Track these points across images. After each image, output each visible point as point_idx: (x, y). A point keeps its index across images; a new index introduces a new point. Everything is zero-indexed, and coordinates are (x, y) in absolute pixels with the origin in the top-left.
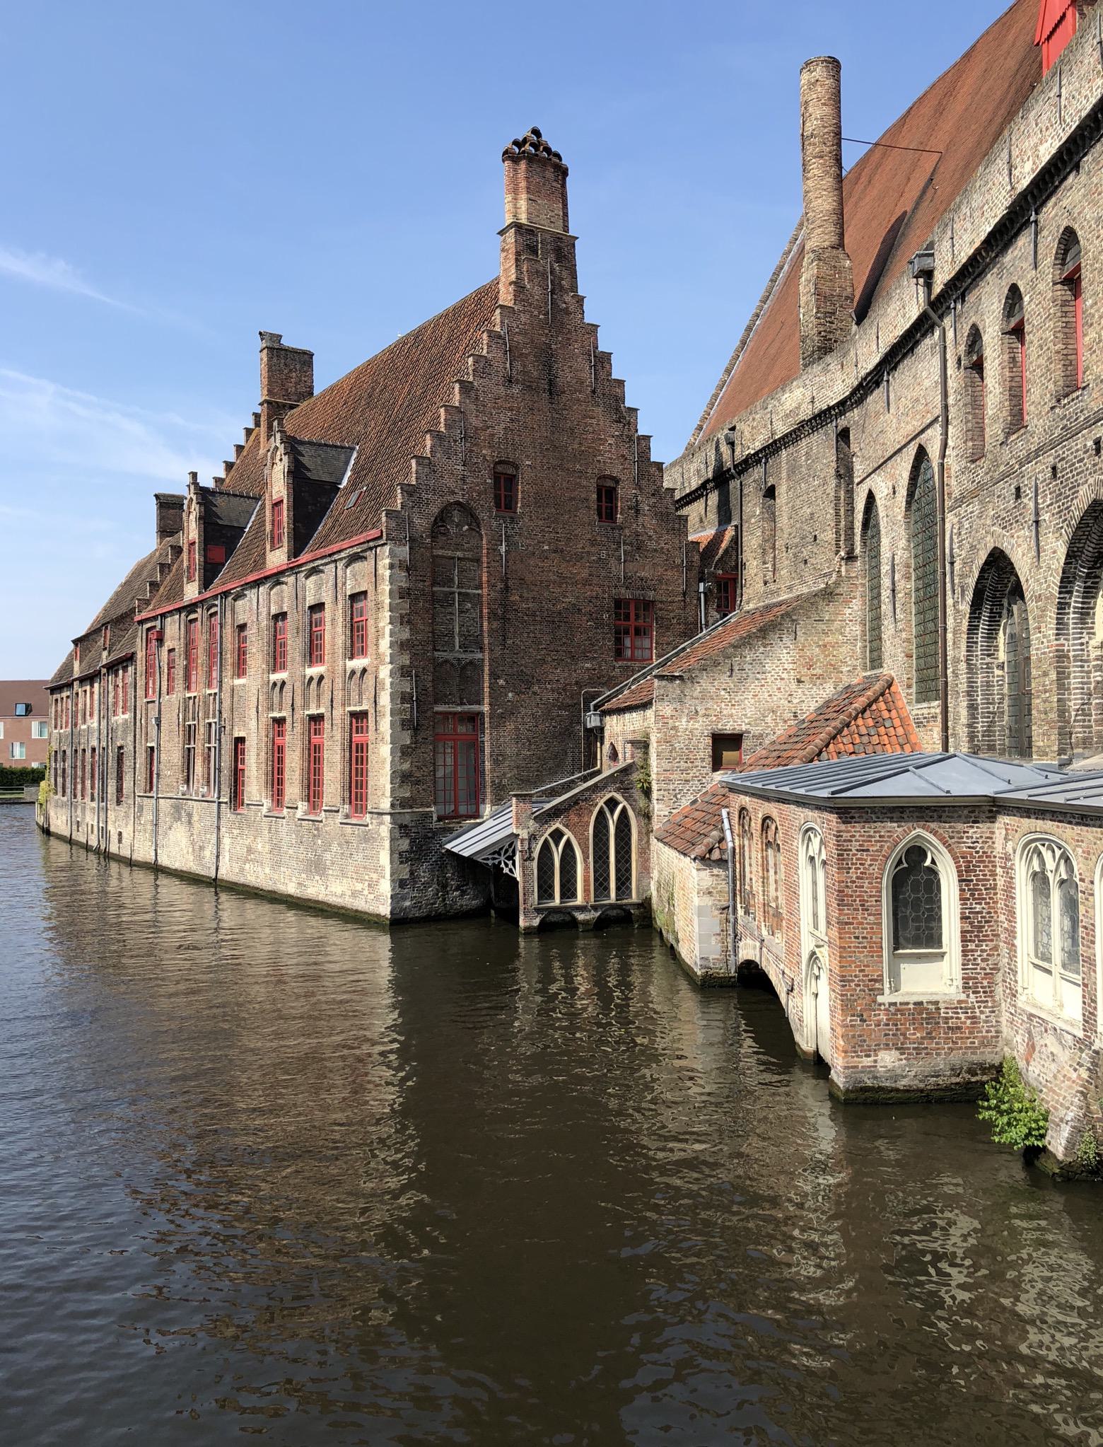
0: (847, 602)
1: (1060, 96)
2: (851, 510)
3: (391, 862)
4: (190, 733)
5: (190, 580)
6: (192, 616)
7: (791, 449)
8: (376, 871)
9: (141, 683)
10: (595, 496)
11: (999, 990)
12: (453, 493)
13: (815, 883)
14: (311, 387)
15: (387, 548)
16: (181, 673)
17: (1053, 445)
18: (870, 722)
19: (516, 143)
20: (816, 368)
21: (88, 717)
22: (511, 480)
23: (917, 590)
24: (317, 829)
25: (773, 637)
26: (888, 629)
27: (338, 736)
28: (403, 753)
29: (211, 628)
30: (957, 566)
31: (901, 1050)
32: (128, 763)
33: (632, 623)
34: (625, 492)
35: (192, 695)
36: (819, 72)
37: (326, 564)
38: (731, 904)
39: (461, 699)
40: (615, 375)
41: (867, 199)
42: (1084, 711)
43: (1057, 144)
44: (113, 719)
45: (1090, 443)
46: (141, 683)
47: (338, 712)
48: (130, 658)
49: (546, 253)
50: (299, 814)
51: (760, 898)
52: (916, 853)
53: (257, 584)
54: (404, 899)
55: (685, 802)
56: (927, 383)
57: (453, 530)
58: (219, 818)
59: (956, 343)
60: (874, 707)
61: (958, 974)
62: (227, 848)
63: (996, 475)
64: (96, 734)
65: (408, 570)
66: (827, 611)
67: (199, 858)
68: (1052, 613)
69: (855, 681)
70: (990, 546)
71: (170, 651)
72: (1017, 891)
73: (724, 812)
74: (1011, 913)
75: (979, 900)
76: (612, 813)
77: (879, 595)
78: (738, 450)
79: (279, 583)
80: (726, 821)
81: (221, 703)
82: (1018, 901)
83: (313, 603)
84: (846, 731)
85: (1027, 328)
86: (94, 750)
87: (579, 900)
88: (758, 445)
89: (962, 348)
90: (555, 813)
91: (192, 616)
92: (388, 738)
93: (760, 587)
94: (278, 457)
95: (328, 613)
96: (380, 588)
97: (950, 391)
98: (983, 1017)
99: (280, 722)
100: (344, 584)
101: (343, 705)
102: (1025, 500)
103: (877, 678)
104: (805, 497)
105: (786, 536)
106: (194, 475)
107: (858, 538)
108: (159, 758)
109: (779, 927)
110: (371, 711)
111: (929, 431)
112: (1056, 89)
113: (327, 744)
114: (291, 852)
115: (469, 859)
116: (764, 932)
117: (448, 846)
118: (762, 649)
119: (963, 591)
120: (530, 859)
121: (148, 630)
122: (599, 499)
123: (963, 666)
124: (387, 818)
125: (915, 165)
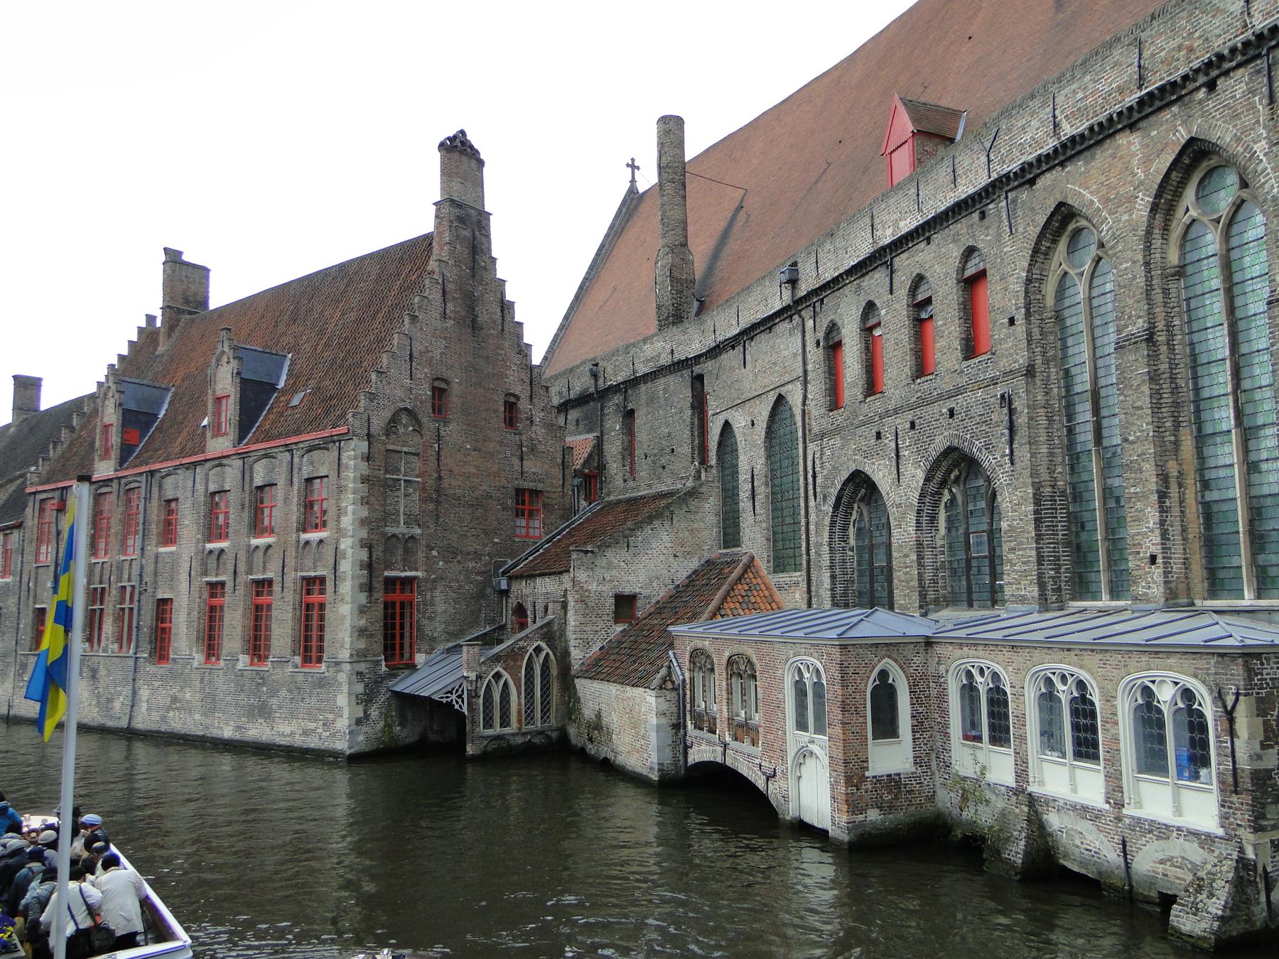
3: (349, 705)
5: (105, 456)
6: (104, 490)
11: (934, 764)
15: (353, 444)
19: (449, 138)
24: (262, 678)
25: (657, 523)
29: (129, 501)
30: (819, 480)
31: (881, 808)
34: (524, 405)
35: (101, 561)
40: (517, 319)
43: (915, 224)
45: (944, 411)
49: (465, 220)
50: (240, 666)
52: (883, 674)
53: (195, 465)
55: (596, 648)
59: (814, 329)
61: (911, 755)
62: (145, 698)
63: (856, 422)
65: (368, 459)
66: (694, 503)
68: (911, 517)
70: (853, 467)
74: (944, 713)
78: (601, 381)
79: (220, 465)
87: (514, 727)
88: (620, 379)
89: (821, 335)
91: (104, 490)
92: (348, 598)
93: (619, 482)
94: (225, 359)
95: (280, 492)
96: (342, 475)
105: (645, 446)
111: (790, 386)
114: (228, 698)
115: (429, 699)
116: (728, 739)
119: (825, 498)
120: (477, 696)
121: (42, 501)
124: (347, 667)
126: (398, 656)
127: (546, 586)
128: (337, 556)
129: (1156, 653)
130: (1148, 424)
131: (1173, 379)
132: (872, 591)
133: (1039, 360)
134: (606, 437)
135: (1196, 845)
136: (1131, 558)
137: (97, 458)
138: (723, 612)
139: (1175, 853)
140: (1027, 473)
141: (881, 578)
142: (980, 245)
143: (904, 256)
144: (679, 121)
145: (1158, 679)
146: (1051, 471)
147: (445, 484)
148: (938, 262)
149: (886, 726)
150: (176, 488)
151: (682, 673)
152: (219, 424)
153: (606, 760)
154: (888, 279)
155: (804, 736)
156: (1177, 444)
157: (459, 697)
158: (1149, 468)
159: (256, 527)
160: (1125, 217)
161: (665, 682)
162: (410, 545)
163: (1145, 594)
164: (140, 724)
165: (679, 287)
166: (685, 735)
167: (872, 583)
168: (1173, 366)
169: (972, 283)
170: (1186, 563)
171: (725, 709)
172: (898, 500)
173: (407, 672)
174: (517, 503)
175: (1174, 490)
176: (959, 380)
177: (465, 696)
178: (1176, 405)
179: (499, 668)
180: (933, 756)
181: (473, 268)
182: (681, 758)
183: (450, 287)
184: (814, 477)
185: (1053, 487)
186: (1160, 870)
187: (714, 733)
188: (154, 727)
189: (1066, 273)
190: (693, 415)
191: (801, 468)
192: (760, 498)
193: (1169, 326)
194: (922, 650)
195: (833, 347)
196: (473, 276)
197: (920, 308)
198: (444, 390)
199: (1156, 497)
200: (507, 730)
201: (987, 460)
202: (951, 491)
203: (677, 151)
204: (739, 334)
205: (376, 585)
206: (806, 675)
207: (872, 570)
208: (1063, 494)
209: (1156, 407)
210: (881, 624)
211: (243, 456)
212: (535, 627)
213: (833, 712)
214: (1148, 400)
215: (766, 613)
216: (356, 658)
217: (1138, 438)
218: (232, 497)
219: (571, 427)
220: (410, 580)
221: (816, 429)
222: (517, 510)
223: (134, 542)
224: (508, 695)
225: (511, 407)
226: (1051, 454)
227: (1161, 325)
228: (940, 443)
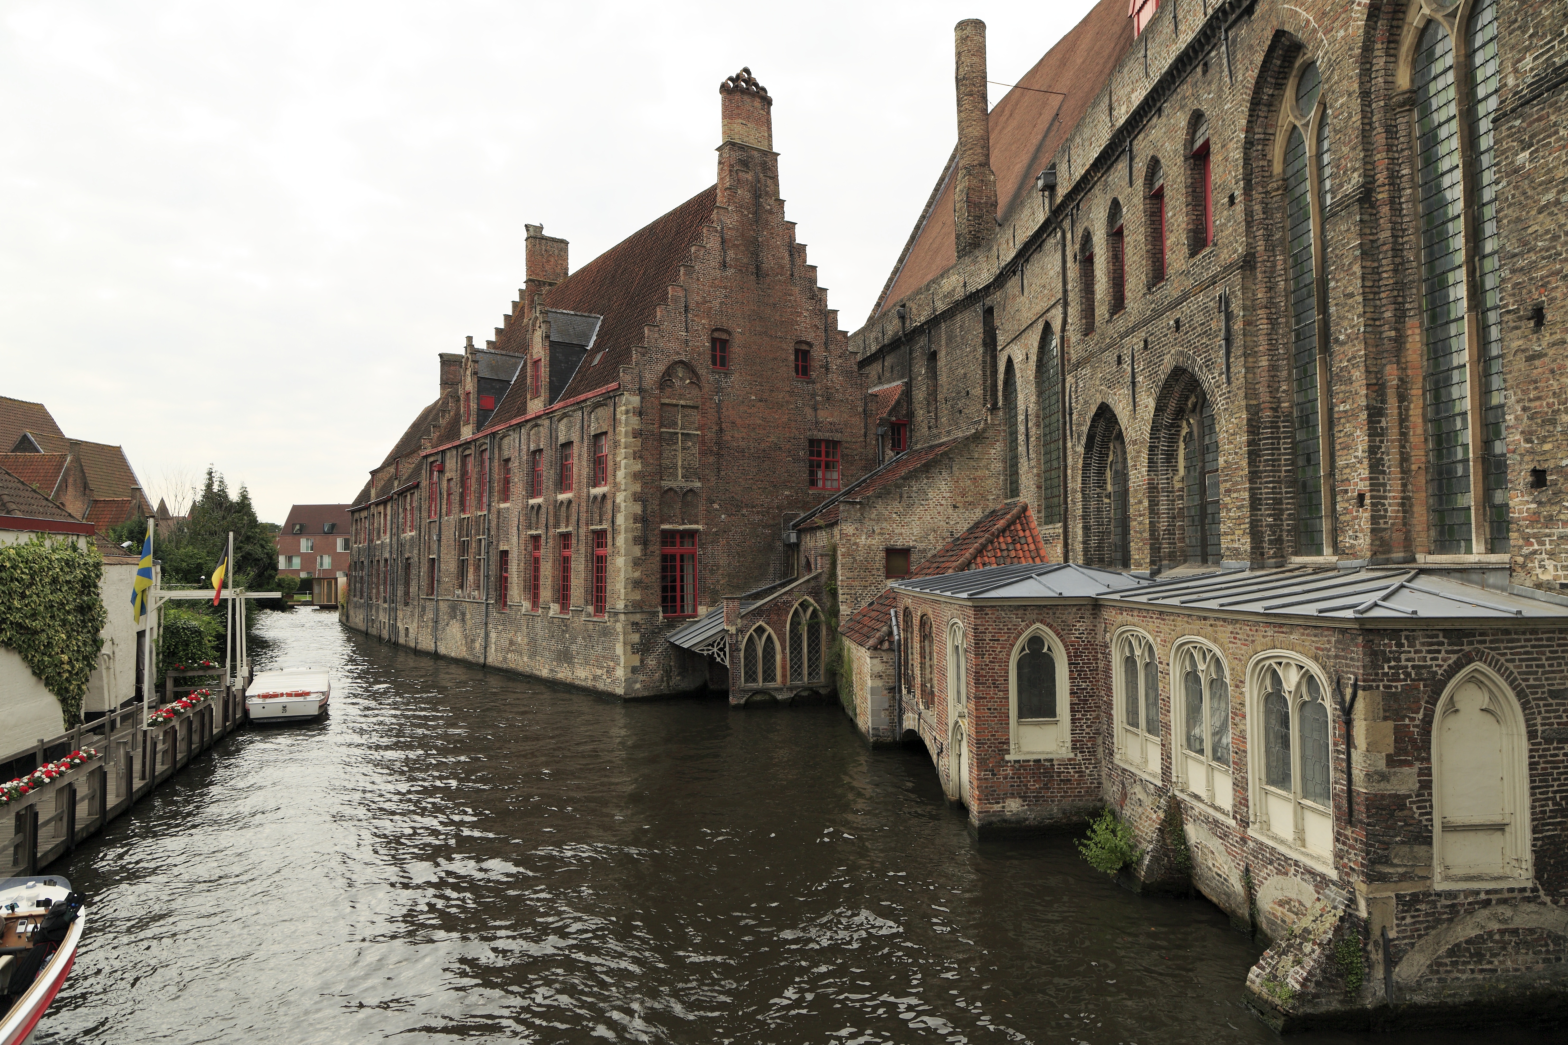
1: (1146, 56)
2: (995, 372)
4: (463, 548)
5: (467, 423)
6: (467, 452)
9: (425, 506)
10: (793, 357)
13: (958, 667)
14: (567, 269)
17: (1146, 322)
18: (1009, 540)
19: (730, 79)
20: (967, 260)
22: (724, 344)
23: (1045, 435)
24: (566, 626)
26: (1024, 466)
27: (583, 550)
28: (635, 564)
29: (482, 462)
30: (1074, 417)
31: (1024, 798)
32: (414, 572)
33: (823, 458)
34: (818, 353)
36: (969, 31)
37: (575, 411)
39: (683, 520)
41: (1009, 128)
42: (1170, 532)
43: (1144, 93)
44: (403, 536)
45: (1172, 322)
46: (425, 506)
48: (417, 486)
51: (918, 680)
52: (1036, 642)
53: (520, 425)
54: (636, 682)
55: (864, 604)
56: (1052, 273)
57: (677, 383)
58: (487, 616)
61: (1068, 738)
62: (493, 641)
64: (388, 549)
65: (640, 414)
67: (471, 648)
68: (1145, 455)
69: (999, 507)
70: (1099, 401)
71: (449, 480)
72: (1114, 672)
73: (892, 612)
74: (1109, 689)
76: (805, 612)
77: (1017, 439)
79: (537, 425)
80: (894, 619)
82: (1114, 679)
83: (563, 441)
84: (990, 547)
85: (1125, 232)
86: (386, 560)
88: (923, 319)
89: (1077, 247)
91: (467, 452)
92: (623, 551)
93: (925, 430)
96: (617, 430)
97: (1070, 280)
98: (1088, 771)
99: (536, 538)
100: (589, 426)
101: (587, 524)
102: (1125, 366)
103: (1015, 504)
106: (470, 339)
107: (1000, 394)
109: (933, 703)
111: (1053, 311)
112: (1143, 52)
114: (544, 644)
115: (688, 650)
116: (922, 707)
117: (672, 640)
118: (925, 481)
119: (1079, 436)
121: (432, 463)
122: (796, 359)
123: (1079, 495)
124: (622, 617)
125: (1044, 104)
126: (678, 608)
127: (821, 539)
129: (1281, 625)
130: (1359, 316)
131: (1397, 250)
133: (1261, 246)
135: (1311, 888)
136: (1339, 498)
139: (1293, 896)
140: (1241, 393)
142: (1204, 108)
143: (1141, 137)
144: (978, 26)
145: (1284, 661)
146: (1273, 390)
147: (727, 437)
148: (1165, 138)
156: (1400, 341)
157: (721, 650)
158: (1358, 374)
160: (1342, 33)
161: (881, 642)
163: (1352, 546)
165: (977, 213)
166: (901, 697)
168: (1397, 232)
169: (1199, 158)
170: (1406, 504)
174: (811, 453)
175: (1392, 405)
176: (1186, 283)
178: (1400, 286)
179: (761, 623)
181: (755, 213)
185: (1275, 410)
186: (1279, 914)
189: (1295, 127)
193: (1393, 177)
194: (1087, 614)
196: (757, 221)
197: (1156, 197)
199: (1364, 415)
200: (771, 685)
201: (1210, 379)
202: (1189, 424)
203: (975, 59)
204: (1016, 257)
208: (1288, 417)
209: (1371, 293)
214: (1359, 282)
216: (630, 609)
217: (1348, 336)
219: (887, 374)
220: (692, 534)
221: (1074, 358)
224: (773, 649)
226: (1273, 368)
227: (1381, 178)
228: (1168, 363)
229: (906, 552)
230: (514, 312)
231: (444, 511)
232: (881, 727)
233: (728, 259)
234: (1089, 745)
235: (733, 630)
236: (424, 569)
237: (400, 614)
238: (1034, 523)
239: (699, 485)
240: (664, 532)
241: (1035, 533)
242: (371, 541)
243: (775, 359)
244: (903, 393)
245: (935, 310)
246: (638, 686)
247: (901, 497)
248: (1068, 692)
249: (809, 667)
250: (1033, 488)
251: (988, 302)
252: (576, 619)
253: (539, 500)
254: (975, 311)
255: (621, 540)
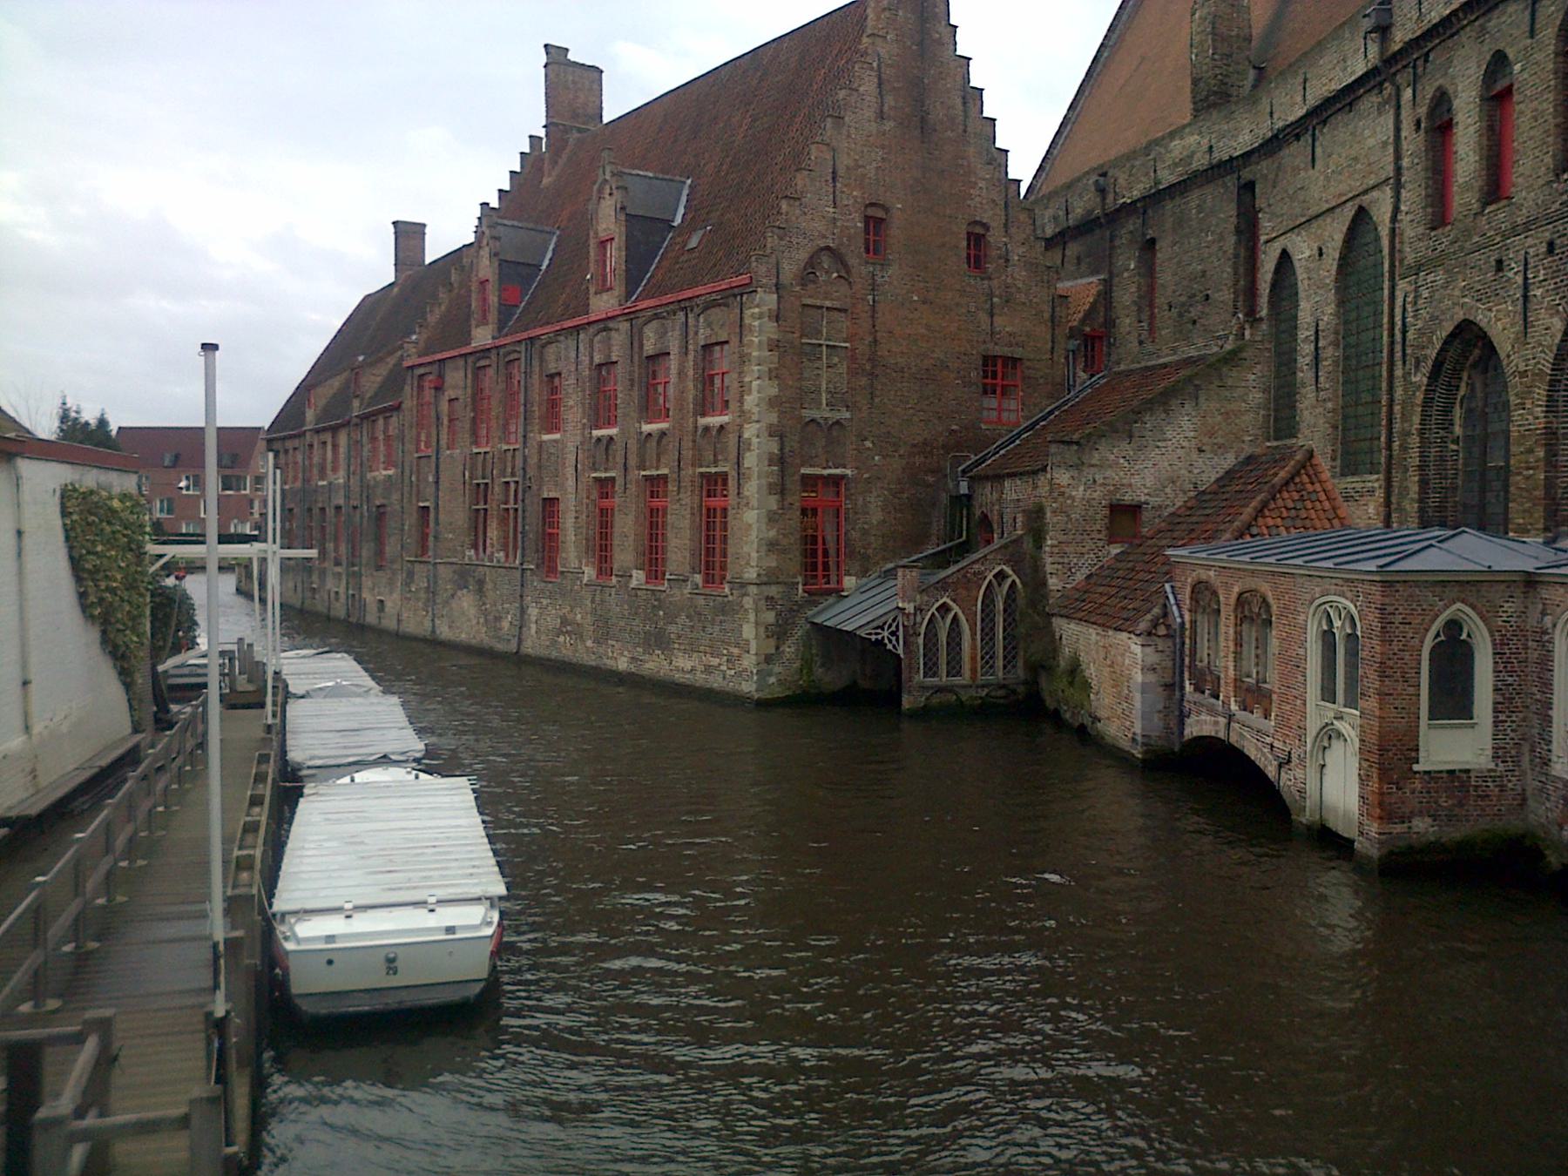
0: (1250, 368)
4: (481, 492)
5: (484, 321)
6: (482, 363)
7: (1178, 201)
8: (737, 645)
9: (410, 435)
10: (965, 243)
11: (1526, 759)
12: (824, 237)
16: (468, 426)
18: (1296, 496)
21: (329, 472)
23: (1346, 358)
25: (1174, 403)
29: (510, 377)
30: (1410, 336)
31: (1435, 817)
32: (391, 524)
33: (999, 381)
34: (996, 237)
35: (482, 450)
38: (1177, 678)
44: (369, 476)
47: (688, 472)
48: (398, 408)
50: (634, 583)
52: (1454, 626)
54: (770, 675)
55: (1080, 577)
60: (1297, 480)
61: (1488, 744)
64: (342, 492)
68: (1541, 392)
69: (1258, 451)
73: (1167, 587)
75: (1511, 673)
78: (1110, 197)
79: (606, 329)
81: (525, 461)
82: (1556, 673)
83: (651, 353)
85: (1516, 97)
88: (1136, 194)
89: (1423, 111)
90: (943, 586)
91: (482, 363)
92: (754, 503)
95: (673, 363)
96: (745, 340)
100: (696, 333)
102: (1510, 275)
104: (1195, 253)
105: (1169, 292)
108: (437, 519)
110: (733, 474)
111: (1375, 194)
113: (671, 507)
114: (622, 624)
115: (851, 634)
116: (1234, 707)
119: (1417, 366)
123: (1415, 440)
124: (753, 590)
127: (1014, 491)
128: (742, 446)
132: (1482, 507)
134: (1116, 280)
137: (473, 323)
138: (1254, 530)
141: (1497, 485)
149: (1452, 698)
150: (558, 359)
151: (1180, 614)
152: (604, 276)
153: (1082, 727)
154: (1527, 13)
155: (1330, 710)
157: (893, 633)
159: (649, 409)
161: (1155, 627)
162: (835, 433)
164: (531, 646)
165: (1226, 51)
166: (1183, 696)
167: (1483, 491)
171: (1231, 665)
172: (1522, 368)
173: (831, 600)
177: (901, 634)
180: (1526, 748)
181: (921, 44)
182: (1175, 729)
183: (888, 72)
184: (1404, 332)
187: (1217, 698)
188: (542, 652)
190: (1238, 242)
191: (1385, 320)
192: (1326, 364)
194: (1518, 592)
195: (1440, 127)
198: (883, 220)
200: (957, 680)
205: (788, 486)
206: (1337, 623)
207: (1483, 475)
210: (1471, 551)
211: (630, 316)
212: (1003, 542)
213: (1370, 677)
215: (1311, 532)
218: (619, 369)
219: (1070, 267)
220: (836, 481)
221: (1410, 258)
222: (985, 385)
223: (517, 427)
224: (960, 634)
225: (977, 239)
229: (1135, 510)
230: (522, 167)
231: (443, 442)
232: (1153, 734)
233: (886, 108)
234: (1513, 752)
235: (910, 608)
236: (411, 520)
237: (367, 582)
238: (1326, 475)
239: (848, 415)
240: (803, 475)
241: (1329, 486)
242: (306, 481)
243: (944, 245)
244: (1099, 294)
245: (1157, 183)
246: (772, 680)
247: (1131, 437)
248: (1491, 688)
249: (1005, 657)
250: (1323, 426)
251: (1246, 174)
252: (675, 591)
253: (613, 431)
254: (1224, 185)
255: (752, 488)
